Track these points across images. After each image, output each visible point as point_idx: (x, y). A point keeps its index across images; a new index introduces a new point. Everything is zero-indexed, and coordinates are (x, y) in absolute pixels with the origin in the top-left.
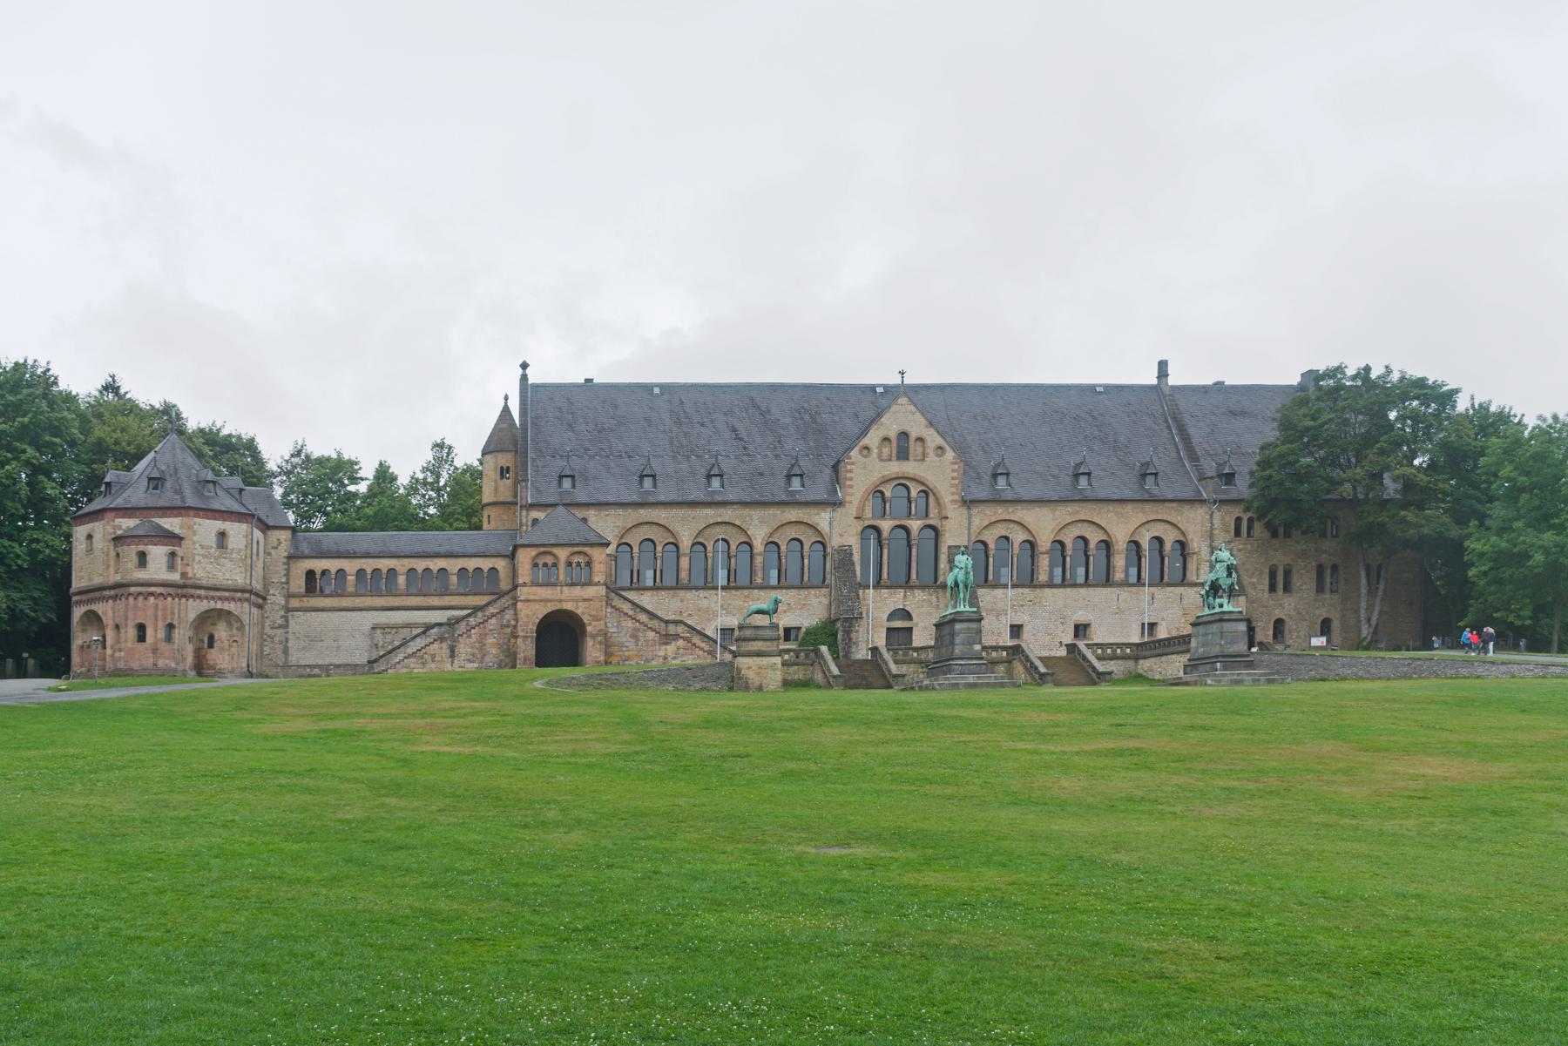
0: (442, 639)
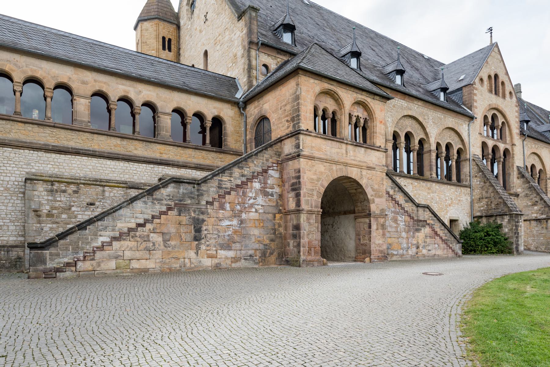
0: (181, 208)
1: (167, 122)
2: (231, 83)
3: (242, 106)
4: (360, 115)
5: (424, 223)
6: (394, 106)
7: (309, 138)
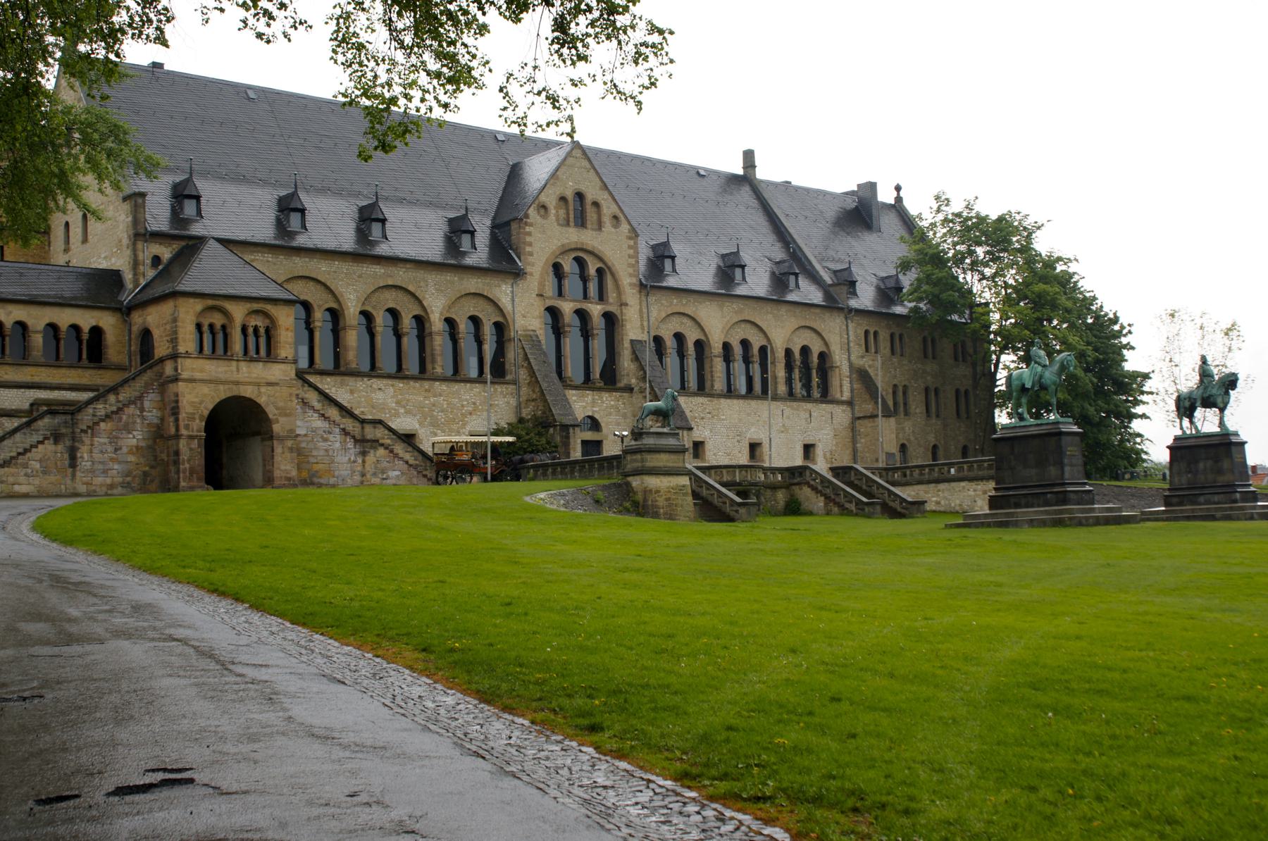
1: (37, 340)
2: (112, 279)
3: (125, 312)
4: (259, 324)
5: (375, 443)
6: (360, 276)
7: (189, 361)
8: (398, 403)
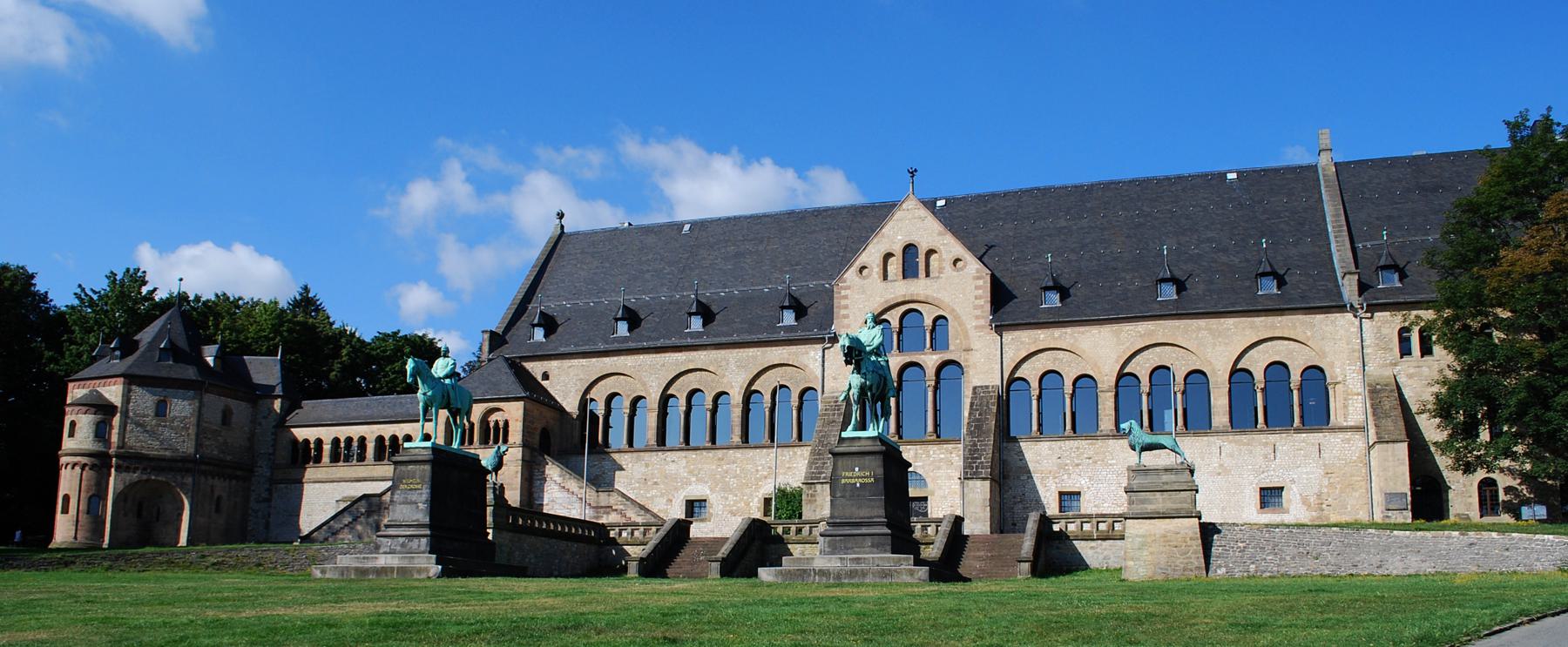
8: (691, 472)
